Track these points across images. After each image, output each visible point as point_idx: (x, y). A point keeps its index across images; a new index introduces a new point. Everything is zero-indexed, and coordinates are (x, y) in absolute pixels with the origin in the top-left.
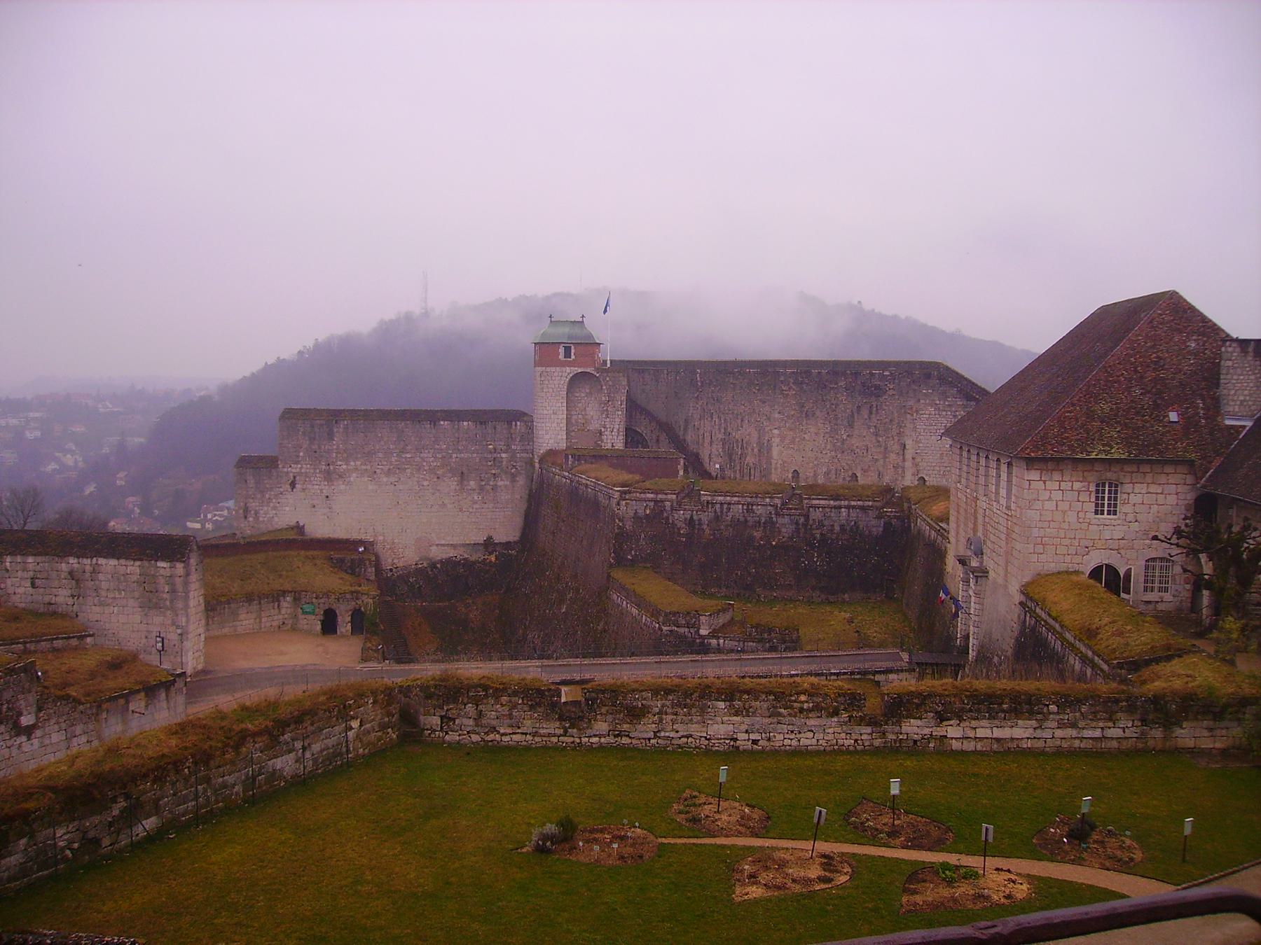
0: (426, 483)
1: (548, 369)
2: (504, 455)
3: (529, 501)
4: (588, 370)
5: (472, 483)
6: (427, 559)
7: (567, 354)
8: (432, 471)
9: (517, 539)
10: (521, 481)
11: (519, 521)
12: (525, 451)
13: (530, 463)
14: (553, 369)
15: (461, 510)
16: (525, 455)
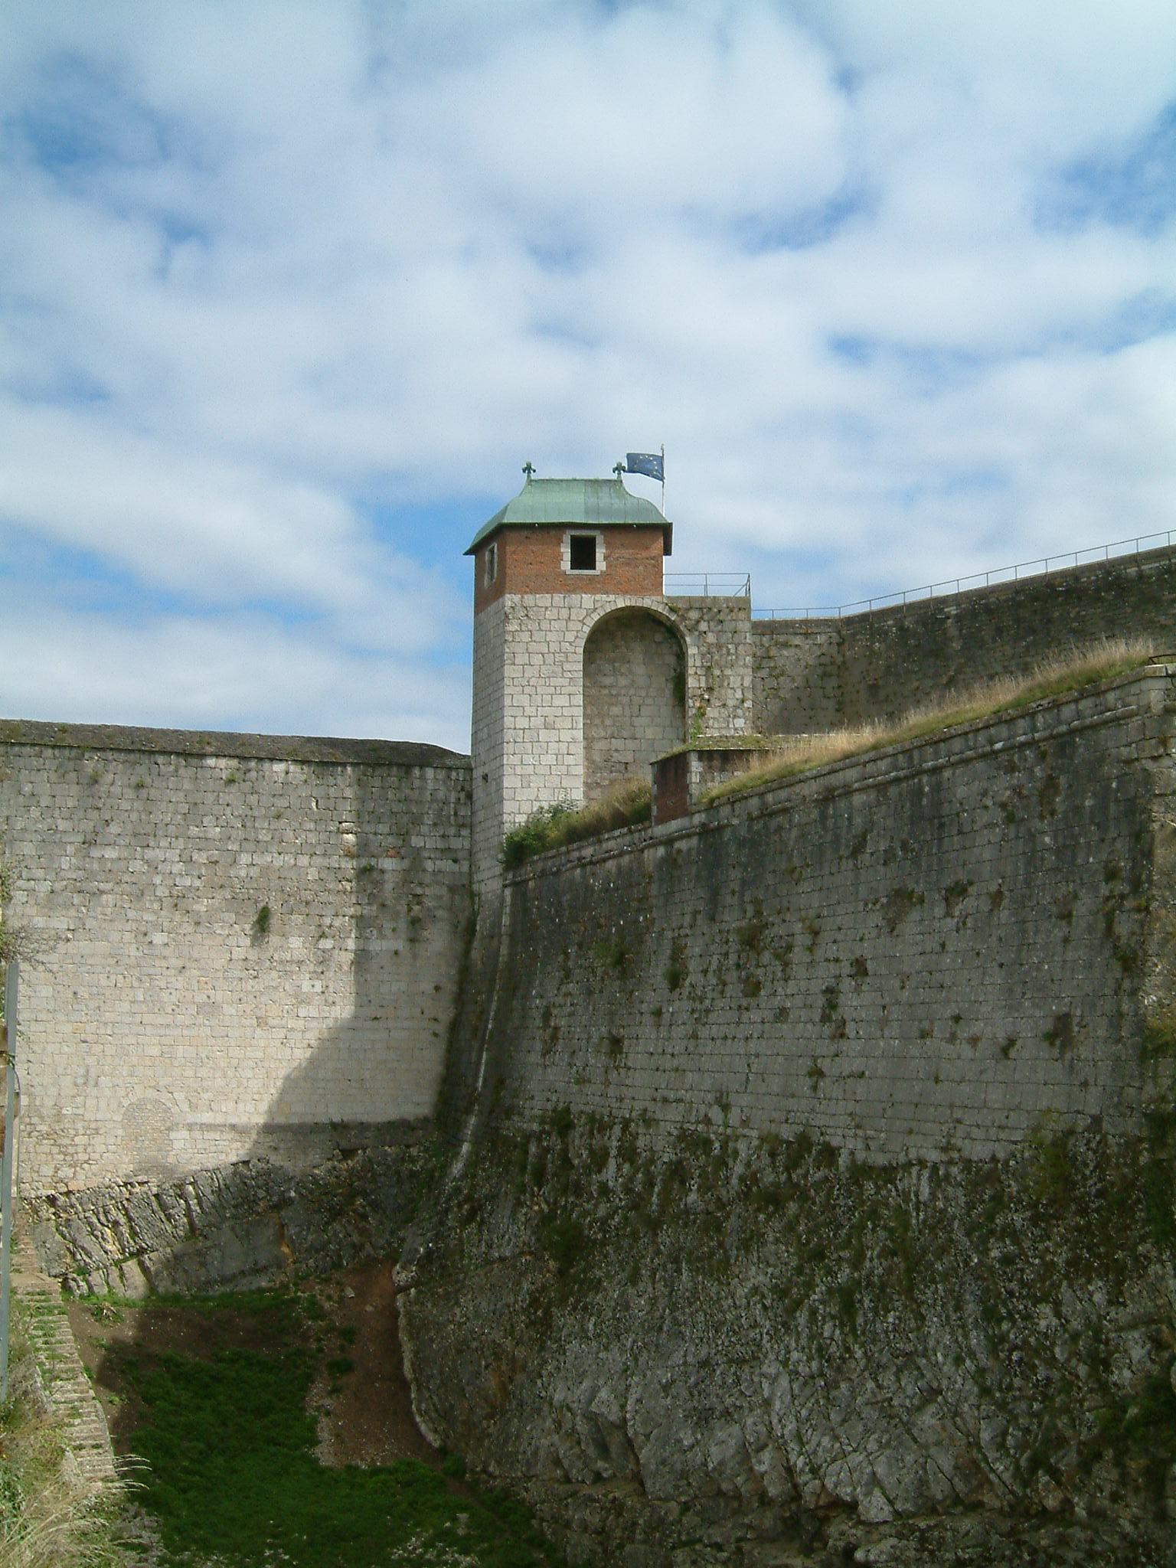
0: (159, 938)
1: (529, 600)
2: (388, 864)
3: (460, 998)
4: (648, 602)
5: (295, 942)
6: (166, 1170)
7: (583, 556)
8: (178, 901)
9: (425, 1110)
10: (438, 940)
11: (431, 1059)
12: (446, 852)
13: (464, 889)
14: (544, 599)
15: (261, 1022)
16: (447, 865)
